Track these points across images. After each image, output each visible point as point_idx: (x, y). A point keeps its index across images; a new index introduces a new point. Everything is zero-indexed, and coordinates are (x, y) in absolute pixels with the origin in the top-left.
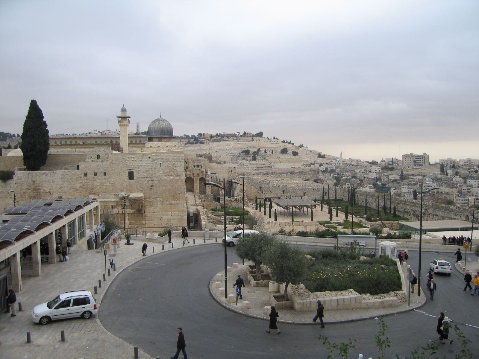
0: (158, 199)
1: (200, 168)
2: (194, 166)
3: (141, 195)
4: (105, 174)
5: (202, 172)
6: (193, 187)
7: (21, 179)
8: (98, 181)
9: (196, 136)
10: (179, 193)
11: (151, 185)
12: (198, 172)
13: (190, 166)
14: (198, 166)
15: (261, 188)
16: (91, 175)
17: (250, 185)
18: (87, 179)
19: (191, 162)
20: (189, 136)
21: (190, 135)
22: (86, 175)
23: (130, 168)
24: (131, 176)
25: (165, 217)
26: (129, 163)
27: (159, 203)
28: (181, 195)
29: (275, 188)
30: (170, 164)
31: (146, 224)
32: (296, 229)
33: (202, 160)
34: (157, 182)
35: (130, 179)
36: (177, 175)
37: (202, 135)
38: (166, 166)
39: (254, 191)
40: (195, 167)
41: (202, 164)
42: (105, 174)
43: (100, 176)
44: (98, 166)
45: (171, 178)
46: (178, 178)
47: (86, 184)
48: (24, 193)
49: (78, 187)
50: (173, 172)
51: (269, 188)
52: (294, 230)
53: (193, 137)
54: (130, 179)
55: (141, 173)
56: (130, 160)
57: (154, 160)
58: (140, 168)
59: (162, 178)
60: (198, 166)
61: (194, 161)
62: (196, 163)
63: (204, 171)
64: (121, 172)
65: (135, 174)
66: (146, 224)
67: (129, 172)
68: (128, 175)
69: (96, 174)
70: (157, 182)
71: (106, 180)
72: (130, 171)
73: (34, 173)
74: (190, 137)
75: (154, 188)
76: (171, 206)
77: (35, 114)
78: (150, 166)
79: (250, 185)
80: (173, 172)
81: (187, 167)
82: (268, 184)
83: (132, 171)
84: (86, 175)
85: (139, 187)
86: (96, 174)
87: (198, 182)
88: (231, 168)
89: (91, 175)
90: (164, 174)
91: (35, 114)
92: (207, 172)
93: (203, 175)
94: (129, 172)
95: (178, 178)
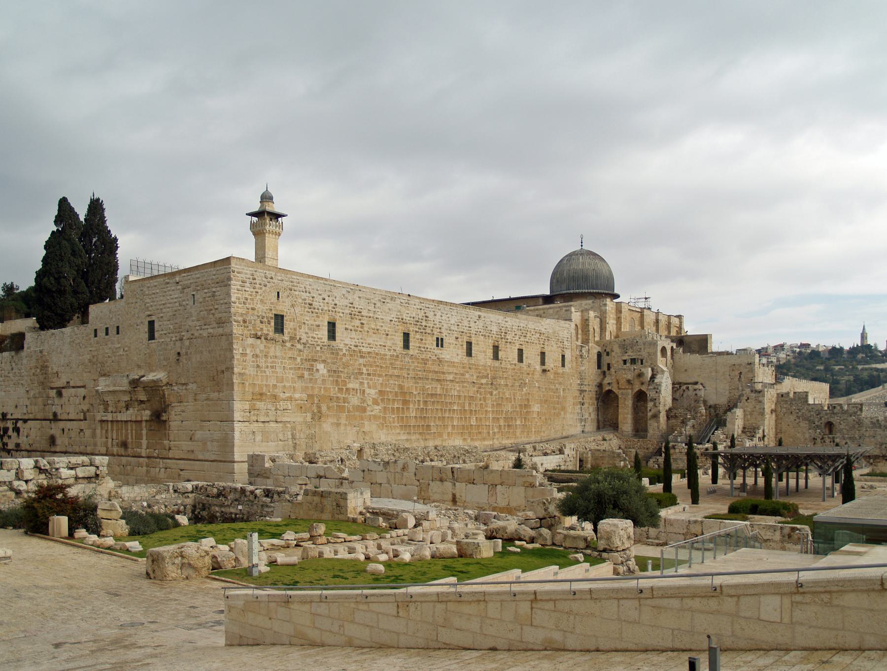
0: (190, 386)
1: (637, 366)
2: (625, 362)
5: (640, 375)
6: (617, 419)
8: (110, 346)
10: (223, 372)
11: (179, 350)
12: (629, 376)
13: (614, 362)
15: (830, 425)
17: (792, 418)
18: (98, 343)
23: (149, 313)
25: (199, 435)
26: (148, 301)
27: (191, 398)
28: (225, 374)
29: (880, 427)
30: (208, 295)
31: (170, 449)
32: (463, 495)
33: (644, 344)
34: (187, 343)
38: (201, 300)
39: (807, 436)
40: (628, 364)
41: (644, 354)
43: (112, 331)
45: (211, 331)
46: (220, 331)
47: (96, 353)
50: (213, 314)
51: (857, 426)
52: (458, 496)
55: (165, 323)
56: (150, 292)
58: (164, 310)
59: (196, 334)
60: (633, 361)
61: (624, 347)
62: (630, 353)
63: (649, 373)
64: (139, 321)
66: (170, 449)
68: (147, 330)
75: (183, 359)
76: (209, 406)
78: (177, 304)
79: (792, 418)
80: (213, 314)
81: (609, 365)
82: (855, 413)
83: (153, 318)
85: (162, 357)
87: (630, 403)
88: (740, 365)
90: (198, 323)
92: (653, 377)
93: (642, 384)
95: (220, 331)
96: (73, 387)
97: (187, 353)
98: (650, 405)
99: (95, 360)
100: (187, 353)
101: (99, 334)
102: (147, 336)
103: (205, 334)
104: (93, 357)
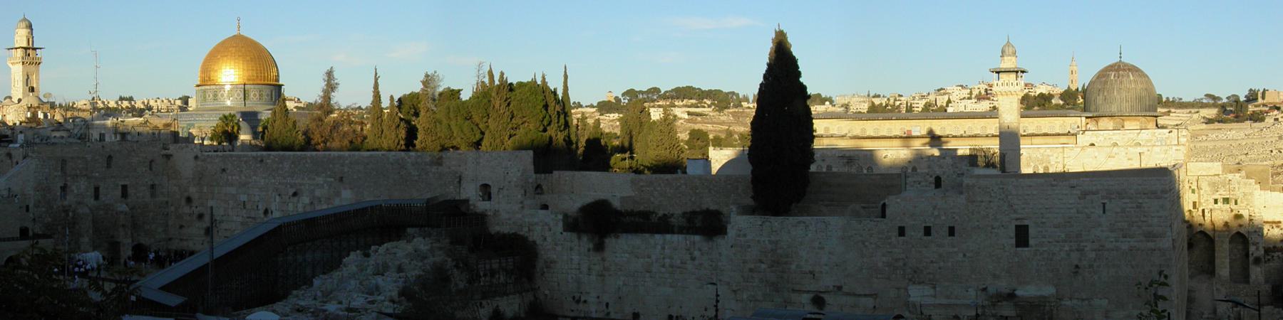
2: (1216, 201)
3: (1049, 291)
4: (952, 231)
7: (745, 235)
9: (1242, 99)
11: (1076, 262)
14: (1226, 201)
16: (915, 234)
19: (1208, 189)
20: (1219, 99)
21: (1224, 95)
22: (902, 231)
24: (1022, 236)
34: (1093, 255)
35: (1018, 245)
36: (1150, 236)
37: (1260, 95)
41: (1238, 194)
42: (952, 231)
44: (935, 208)
48: (751, 270)
49: (880, 264)
53: (1235, 100)
54: (1018, 245)
57: (1085, 194)
60: (1226, 201)
62: (1221, 192)
65: (1032, 231)
67: (1017, 227)
68: (1013, 234)
69: (928, 231)
70: (1093, 255)
71: (954, 247)
72: (1019, 223)
73: (776, 221)
74: (1225, 100)
77: (783, 67)
83: (1026, 222)
84: (902, 231)
86: (928, 231)
87: (1226, 246)
89: (915, 234)
91: (783, 67)
94: (1017, 227)
96: (848, 294)
97: (1091, 266)
98: (1252, 249)
99: (901, 263)
100: (1091, 266)
101: (908, 232)
102: (1013, 241)
103: (1125, 247)
104: (897, 260)
